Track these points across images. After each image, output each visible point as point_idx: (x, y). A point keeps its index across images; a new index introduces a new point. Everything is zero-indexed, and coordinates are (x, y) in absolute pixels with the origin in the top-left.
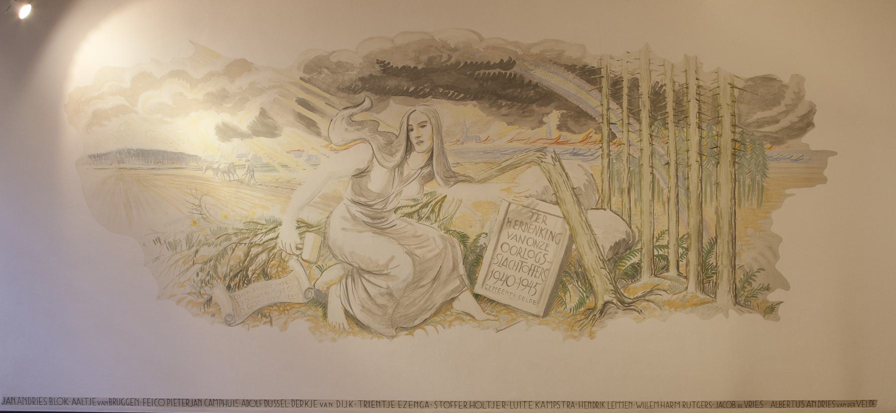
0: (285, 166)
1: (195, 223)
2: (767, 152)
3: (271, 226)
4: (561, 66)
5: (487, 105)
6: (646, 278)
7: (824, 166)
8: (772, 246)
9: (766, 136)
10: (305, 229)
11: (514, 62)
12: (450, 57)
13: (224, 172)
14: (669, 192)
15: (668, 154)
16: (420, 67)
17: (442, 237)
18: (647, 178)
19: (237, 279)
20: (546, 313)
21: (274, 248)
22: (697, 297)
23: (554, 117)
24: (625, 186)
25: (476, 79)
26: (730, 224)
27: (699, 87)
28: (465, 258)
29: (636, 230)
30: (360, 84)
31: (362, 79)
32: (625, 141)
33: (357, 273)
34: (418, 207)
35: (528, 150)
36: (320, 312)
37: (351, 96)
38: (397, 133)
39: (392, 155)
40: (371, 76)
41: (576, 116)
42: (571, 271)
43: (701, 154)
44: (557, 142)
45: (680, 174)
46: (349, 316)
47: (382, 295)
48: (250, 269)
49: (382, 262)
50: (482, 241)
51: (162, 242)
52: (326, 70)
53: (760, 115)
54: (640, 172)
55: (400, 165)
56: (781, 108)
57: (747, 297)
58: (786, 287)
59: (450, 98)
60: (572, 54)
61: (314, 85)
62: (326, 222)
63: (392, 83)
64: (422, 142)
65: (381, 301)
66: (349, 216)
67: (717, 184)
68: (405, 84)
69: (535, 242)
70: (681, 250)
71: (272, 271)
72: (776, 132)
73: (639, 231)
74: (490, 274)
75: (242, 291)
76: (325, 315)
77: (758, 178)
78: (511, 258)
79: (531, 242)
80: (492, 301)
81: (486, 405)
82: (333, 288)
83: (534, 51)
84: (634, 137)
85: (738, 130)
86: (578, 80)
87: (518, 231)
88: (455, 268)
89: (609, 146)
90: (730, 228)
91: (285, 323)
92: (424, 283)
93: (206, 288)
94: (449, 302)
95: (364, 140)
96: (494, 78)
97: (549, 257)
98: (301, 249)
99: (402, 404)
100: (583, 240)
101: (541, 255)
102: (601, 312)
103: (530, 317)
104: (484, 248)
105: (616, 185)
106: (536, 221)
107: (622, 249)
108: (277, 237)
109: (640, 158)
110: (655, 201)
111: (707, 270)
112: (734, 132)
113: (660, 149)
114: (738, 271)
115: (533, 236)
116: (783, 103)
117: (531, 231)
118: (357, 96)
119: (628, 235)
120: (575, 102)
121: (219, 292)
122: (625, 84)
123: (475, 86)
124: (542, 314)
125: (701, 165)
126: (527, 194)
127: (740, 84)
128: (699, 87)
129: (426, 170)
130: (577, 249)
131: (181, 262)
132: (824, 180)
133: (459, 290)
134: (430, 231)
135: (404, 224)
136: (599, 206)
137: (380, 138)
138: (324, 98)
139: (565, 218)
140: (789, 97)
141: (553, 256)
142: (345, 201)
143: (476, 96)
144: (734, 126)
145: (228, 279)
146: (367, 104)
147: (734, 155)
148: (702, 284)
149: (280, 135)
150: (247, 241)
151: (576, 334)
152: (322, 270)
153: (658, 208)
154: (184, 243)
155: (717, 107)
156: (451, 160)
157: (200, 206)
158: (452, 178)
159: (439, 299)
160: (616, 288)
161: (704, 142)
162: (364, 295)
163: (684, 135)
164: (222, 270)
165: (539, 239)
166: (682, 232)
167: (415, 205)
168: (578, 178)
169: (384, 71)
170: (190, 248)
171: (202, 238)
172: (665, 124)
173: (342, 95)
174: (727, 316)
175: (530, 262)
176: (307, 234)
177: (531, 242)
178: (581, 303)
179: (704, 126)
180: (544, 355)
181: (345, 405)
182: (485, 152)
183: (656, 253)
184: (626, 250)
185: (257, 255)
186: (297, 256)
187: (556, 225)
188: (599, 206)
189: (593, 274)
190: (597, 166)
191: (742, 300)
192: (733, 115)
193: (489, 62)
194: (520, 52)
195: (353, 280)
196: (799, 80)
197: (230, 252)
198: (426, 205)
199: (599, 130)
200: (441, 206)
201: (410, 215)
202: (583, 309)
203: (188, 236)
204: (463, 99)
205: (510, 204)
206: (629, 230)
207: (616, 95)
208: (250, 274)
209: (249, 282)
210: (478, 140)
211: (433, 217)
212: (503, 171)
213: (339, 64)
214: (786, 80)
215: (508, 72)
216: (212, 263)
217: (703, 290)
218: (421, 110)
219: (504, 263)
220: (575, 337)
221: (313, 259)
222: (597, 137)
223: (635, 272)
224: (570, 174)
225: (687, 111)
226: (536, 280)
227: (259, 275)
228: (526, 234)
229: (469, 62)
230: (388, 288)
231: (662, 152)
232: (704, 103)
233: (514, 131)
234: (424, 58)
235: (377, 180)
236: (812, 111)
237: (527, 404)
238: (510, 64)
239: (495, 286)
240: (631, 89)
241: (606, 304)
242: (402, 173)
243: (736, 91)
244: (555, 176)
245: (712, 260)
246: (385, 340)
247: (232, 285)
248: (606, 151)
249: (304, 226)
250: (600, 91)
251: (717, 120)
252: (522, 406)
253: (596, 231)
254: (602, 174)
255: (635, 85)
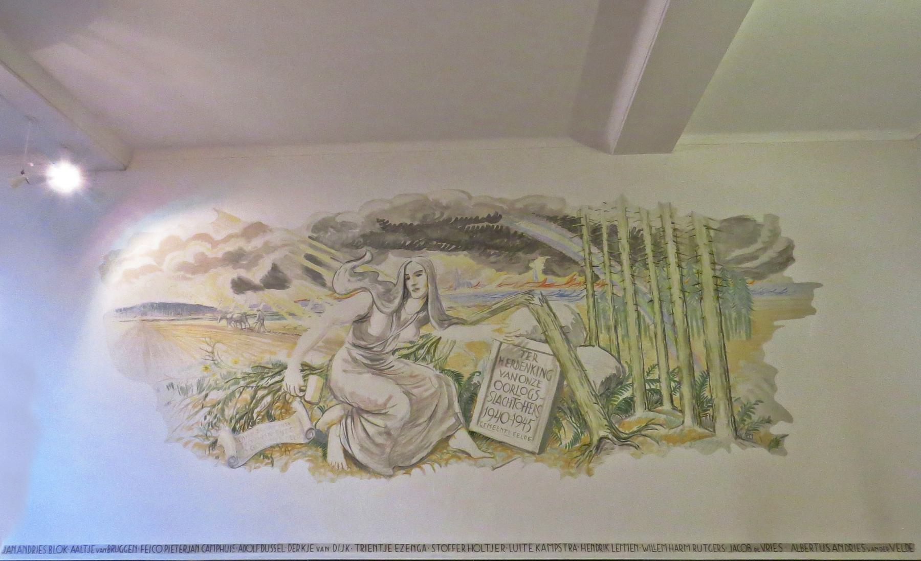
0: (292, 314)
1: (206, 368)
2: (751, 287)
3: (277, 370)
4: (544, 217)
5: (477, 254)
6: (640, 413)
7: (811, 297)
8: (769, 376)
9: (747, 272)
10: (308, 372)
11: (501, 216)
12: (442, 214)
13: (236, 321)
14: (655, 327)
15: (651, 292)
16: (415, 224)
17: (438, 377)
18: (632, 316)
19: (242, 421)
20: (542, 449)
21: (279, 390)
22: (695, 431)
23: (539, 263)
24: (612, 323)
25: (467, 232)
26: (721, 357)
27: (675, 230)
28: (460, 396)
29: (625, 365)
30: (362, 240)
31: (363, 236)
32: (608, 281)
33: (356, 412)
34: (414, 349)
35: (517, 293)
36: (320, 452)
37: (354, 251)
38: (395, 282)
39: (390, 301)
40: (371, 232)
41: (560, 261)
42: (563, 406)
43: (683, 291)
44: (544, 285)
45: (665, 311)
46: (349, 456)
47: (380, 434)
48: (256, 411)
49: (381, 401)
50: (475, 380)
51: (175, 387)
52: (332, 230)
53: (738, 252)
54: (625, 311)
55: (398, 311)
56: (758, 245)
57: (748, 430)
58: (788, 418)
59: (443, 250)
60: (553, 207)
61: (321, 242)
62: (328, 365)
63: (390, 238)
64: (418, 289)
65: (380, 440)
66: (350, 360)
67: (703, 318)
68: (401, 238)
69: (527, 380)
70: (673, 384)
71: (275, 412)
72: (757, 268)
73: (630, 367)
74: (484, 411)
75: (246, 433)
76: (325, 455)
77: (744, 311)
78: (504, 395)
79: (523, 379)
80: (487, 439)
81: (485, 548)
82: (333, 428)
83: (519, 205)
84: (616, 278)
85: (718, 267)
86: (559, 229)
87: (510, 369)
88: (450, 406)
89: (593, 287)
90: (721, 360)
91: (286, 464)
92: (421, 420)
93: (212, 431)
94: (445, 440)
95: (365, 289)
96: (483, 230)
97: (542, 394)
98: (304, 391)
99: (399, 547)
100: (574, 376)
101: (534, 392)
102: (598, 448)
103: (527, 454)
104: (478, 386)
105: (603, 322)
106: (527, 358)
107: (612, 384)
108: (282, 380)
109: (624, 296)
110: (643, 336)
111: (703, 403)
112: (714, 270)
113: (641, 286)
114: (735, 404)
115: (525, 373)
116: (760, 240)
117: (523, 368)
118: (359, 251)
119: (618, 370)
120: (558, 249)
121: (224, 435)
122: (604, 231)
123: (466, 238)
124: (537, 451)
125: (684, 301)
126: (518, 333)
127: (715, 225)
128: (675, 230)
129: (422, 315)
130: (568, 385)
131: (190, 407)
132: (813, 311)
133: (454, 428)
134: (426, 371)
135: (401, 365)
136: (588, 343)
137: (379, 287)
138: (330, 253)
139: (554, 355)
140: (765, 234)
141: (546, 391)
142: (347, 345)
143: (466, 247)
144: (714, 263)
145: (233, 422)
146: (368, 257)
147: (716, 290)
148: (698, 418)
149: (288, 287)
150: (254, 385)
151: (573, 471)
152: (323, 411)
153: (646, 344)
154: (195, 388)
155: (695, 247)
156: (445, 304)
157: (213, 353)
158: (446, 321)
159: (435, 437)
160: (610, 422)
161: (685, 280)
162: (363, 435)
163: (664, 274)
164: (229, 412)
165: (531, 376)
166: (673, 365)
167: (412, 347)
168: (566, 318)
169: (383, 228)
170: (200, 393)
171: (212, 382)
172: (646, 265)
173: (345, 250)
174: (729, 451)
175: (523, 399)
176: (311, 376)
177: (523, 379)
178: (576, 439)
179: (683, 265)
180: (532, 497)
181: (341, 549)
182: (477, 296)
183: (648, 387)
184: (617, 385)
185: (263, 398)
186: (300, 397)
187: (546, 362)
188: (588, 343)
189: (586, 409)
190: (582, 305)
191: (743, 433)
192: (711, 254)
193: (477, 217)
194: (505, 207)
195: (353, 419)
196: (773, 219)
197: (237, 395)
198: (422, 347)
199: (582, 273)
200: (436, 347)
201: (407, 356)
202: (578, 445)
203: (199, 381)
204: (454, 250)
205: (501, 343)
206: (619, 365)
207: (596, 238)
208: (255, 416)
209: (254, 424)
210: (470, 286)
211: (428, 358)
212: (494, 313)
213: (344, 224)
214: (760, 219)
215: (495, 225)
216: (220, 406)
217: (700, 424)
218: (416, 261)
219: (498, 401)
220: (572, 475)
221: (315, 400)
222: (581, 279)
223: (628, 406)
224: (558, 314)
225: (666, 251)
226: (529, 417)
227: (263, 416)
228: (517, 371)
229: (459, 217)
230: (386, 427)
231: (645, 290)
232: (681, 243)
233: (503, 277)
234: (419, 215)
235: (376, 325)
236: (790, 247)
237: (527, 547)
238: (497, 218)
239: (491, 423)
240: (610, 235)
241: (601, 439)
242: (399, 318)
243: (712, 233)
244: (544, 317)
245: (706, 393)
246: (383, 480)
247: (238, 426)
248: (591, 292)
249: (307, 369)
250: (581, 237)
251: (697, 259)
252: (522, 549)
253: (586, 367)
254: (588, 312)
255: (613, 231)
